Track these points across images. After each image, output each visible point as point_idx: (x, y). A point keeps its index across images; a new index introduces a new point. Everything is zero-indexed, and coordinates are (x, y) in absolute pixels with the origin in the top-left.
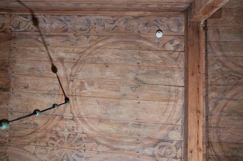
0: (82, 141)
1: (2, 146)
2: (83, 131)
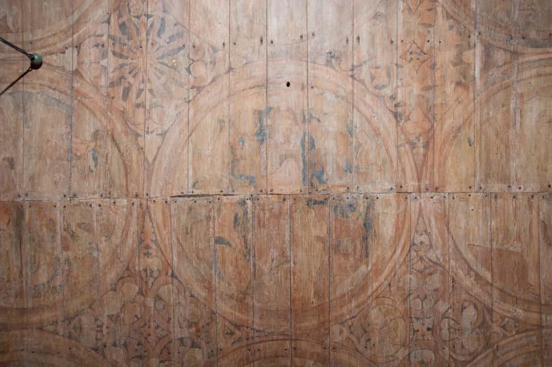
0: (126, 23)
1: (149, 213)
2: (103, 22)
